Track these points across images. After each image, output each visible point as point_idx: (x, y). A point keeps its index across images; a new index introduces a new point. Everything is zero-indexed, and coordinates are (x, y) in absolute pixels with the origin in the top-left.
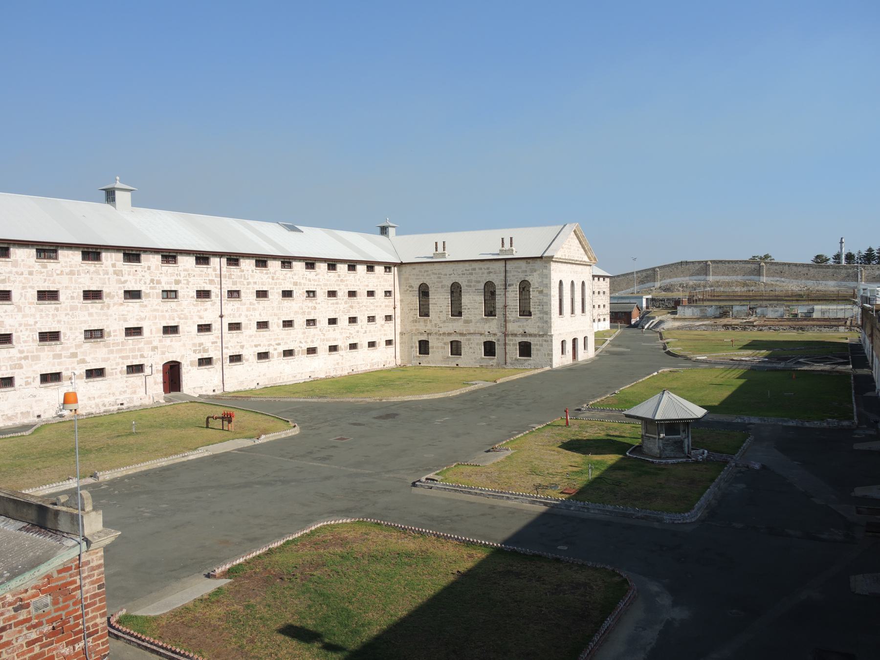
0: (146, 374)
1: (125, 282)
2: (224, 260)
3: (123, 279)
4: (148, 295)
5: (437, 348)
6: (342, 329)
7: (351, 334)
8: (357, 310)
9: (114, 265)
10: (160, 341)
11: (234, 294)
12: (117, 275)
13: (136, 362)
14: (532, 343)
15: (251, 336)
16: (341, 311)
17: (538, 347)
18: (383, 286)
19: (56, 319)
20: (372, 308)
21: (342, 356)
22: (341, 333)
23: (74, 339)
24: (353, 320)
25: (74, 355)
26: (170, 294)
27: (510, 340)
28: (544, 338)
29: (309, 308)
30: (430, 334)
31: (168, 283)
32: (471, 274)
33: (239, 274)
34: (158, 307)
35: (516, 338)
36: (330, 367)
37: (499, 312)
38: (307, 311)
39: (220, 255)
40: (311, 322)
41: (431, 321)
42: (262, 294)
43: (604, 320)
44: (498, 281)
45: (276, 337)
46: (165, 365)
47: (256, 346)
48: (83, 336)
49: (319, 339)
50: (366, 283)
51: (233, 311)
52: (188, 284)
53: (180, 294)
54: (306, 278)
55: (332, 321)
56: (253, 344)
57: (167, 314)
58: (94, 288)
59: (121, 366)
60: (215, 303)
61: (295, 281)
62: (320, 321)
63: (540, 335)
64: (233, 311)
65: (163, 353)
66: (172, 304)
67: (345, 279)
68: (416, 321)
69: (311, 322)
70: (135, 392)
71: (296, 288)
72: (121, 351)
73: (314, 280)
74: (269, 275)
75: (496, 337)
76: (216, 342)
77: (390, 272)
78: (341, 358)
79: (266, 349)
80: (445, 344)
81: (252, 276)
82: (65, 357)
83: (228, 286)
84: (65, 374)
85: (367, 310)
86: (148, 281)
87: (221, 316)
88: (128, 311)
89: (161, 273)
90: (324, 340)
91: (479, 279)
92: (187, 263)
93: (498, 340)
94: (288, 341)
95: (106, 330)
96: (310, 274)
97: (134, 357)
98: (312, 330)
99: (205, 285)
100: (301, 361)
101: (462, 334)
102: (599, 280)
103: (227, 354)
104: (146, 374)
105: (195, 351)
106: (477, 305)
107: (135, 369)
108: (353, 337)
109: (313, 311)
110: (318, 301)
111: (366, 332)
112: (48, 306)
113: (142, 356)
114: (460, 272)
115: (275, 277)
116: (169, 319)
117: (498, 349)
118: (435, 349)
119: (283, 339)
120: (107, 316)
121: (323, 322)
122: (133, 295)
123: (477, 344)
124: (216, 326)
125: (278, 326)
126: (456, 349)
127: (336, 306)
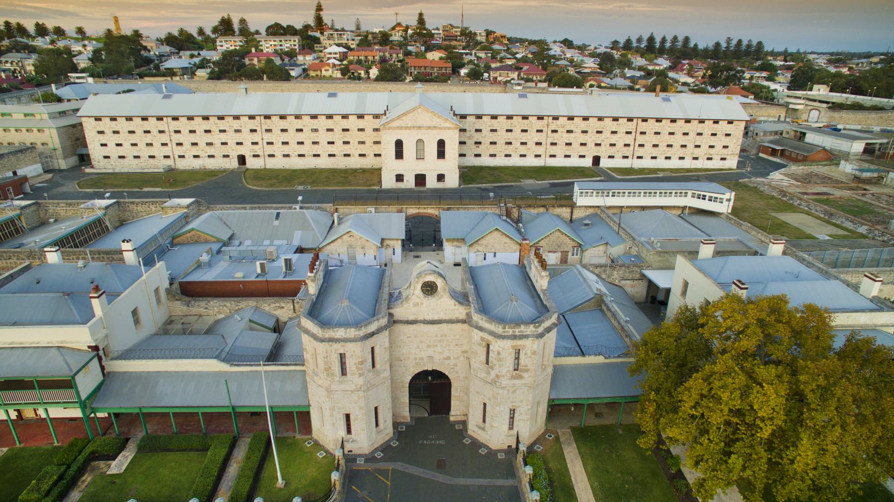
2: (262, 117)
83: (265, 127)
112: (193, 135)
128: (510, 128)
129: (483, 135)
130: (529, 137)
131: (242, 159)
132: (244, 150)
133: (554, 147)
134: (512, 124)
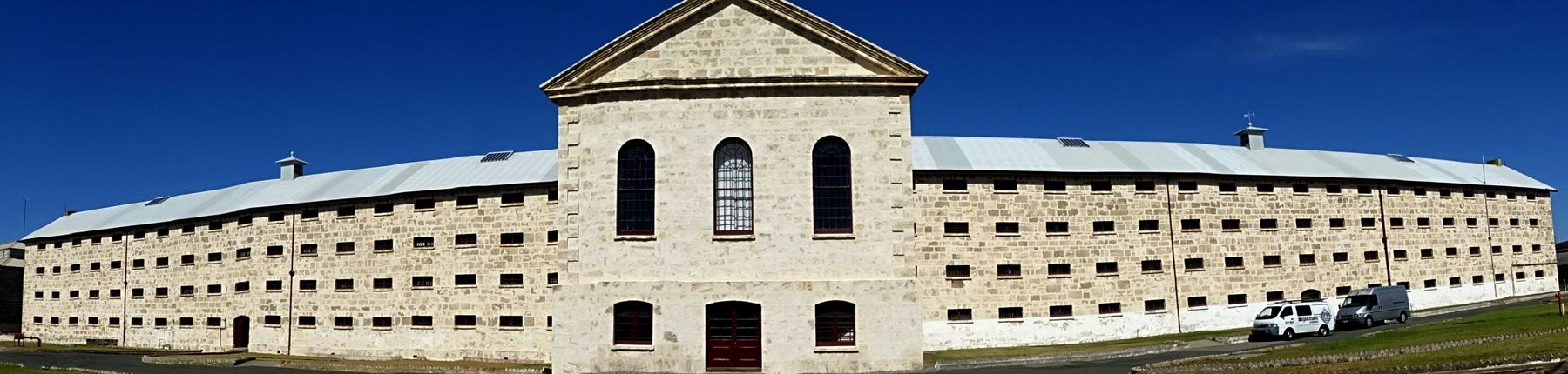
6: (484, 292)
7: (507, 301)
8: (521, 263)
13: (214, 316)
15: (327, 296)
16: (483, 266)
21: (483, 334)
29: (418, 261)
33: (316, 226)
36: (455, 348)
38: (414, 265)
45: (363, 299)
46: (236, 320)
47: (333, 308)
49: (437, 305)
50: (547, 220)
52: (260, 241)
54: (415, 221)
56: (330, 306)
61: (395, 226)
62: (439, 279)
67: (495, 215)
70: (212, 342)
71: (396, 236)
73: (431, 223)
74: (356, 223)
76: (285, 300)
78: (479, 335)
79: (347, 314)
81: (332, 227)
85: (548, 263)
87: (292, 274)
90: (445, 307)
94: (382, 306)
97: (214, 311)
99: (276, 240)
100: (402, 332)
103: (296, 314)
105: (262, 308)
108: (510, 306)
110: (435, 252)
111: (542, 299)
113: (219, 311)
115: (365, 226)
119: (373, 303)
124: (285, 283)
125: (367, 285)
128: (1058, 219)
129: (974, 243)
130: (1120, 246)
131: (242, 325)
132: (252, 306)
133: (1196, 274)
134: (1063, 204)
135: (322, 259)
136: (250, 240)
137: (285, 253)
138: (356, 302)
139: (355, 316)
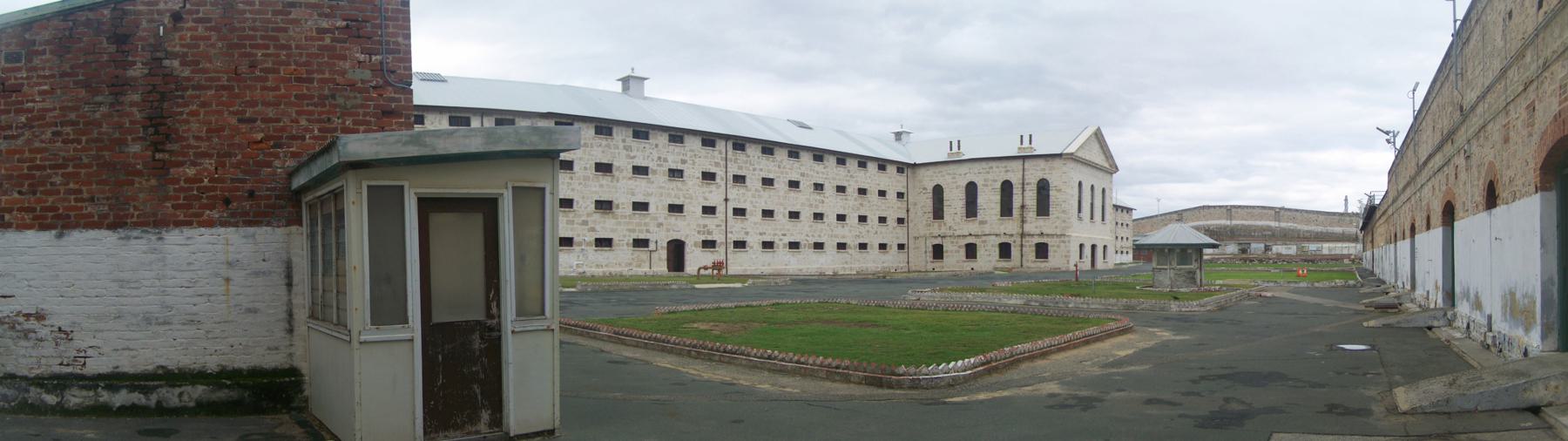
0: (650, 249)
1: (634, 157)
3: (632, 154)
4: (655, 172)
5: (951, 252)
9: (624, 141)
10: (665, 218)
11: (739, 179)
12: (627, 150)
13: (642, 236)
14: (1050, 244)
15: (755, 224)
17: (1055, 248)
18: (896, 186)
19: (570, 187)
20: (883, 208)
22: (850, 231)
23: (586, 208)
24: (863, 219)
25: (585, 223)
26: (676, 174)
27: (1028, 241)
28: (1062, 239)
30: (944, 237)
31: (674, 162)
32: (988, 173)
34: (664, 185)
35: (1033, 239)
37: (1016, 212)
39: (726, 137)
40: (818, 216)
41: (945, 224)
42: (768, 182)
43: (1127, 252)
44: (1015, 179)
46: (669, 243)
47: (761, 234)
48: (593, 206)
51: (738, 197)
53: (685, 174)
55: (841, 218)
56: (758, 232)
57: (673, 193)
58: (605, 161)
59: (627, 238)
60: (720, 186)
63: (1057, 235)
64: (738, 197)
65: (668, 230)
66: (677, 184)
68: (930, 226)
69: (818, 216)
72: (628, 223)
73: (823, 173)
75: (1012, 239)
77: (903, 172)
80: (959, 247)
82: (577, 223)
83: (734, 170)
84: (576, 239)
86: (656, 159)
87: (726, 200)
88: (637, 186)
89: (668, 152)
91: (996, 178)
92: (694, 144)
93: (1014, 242)
95: (615, 202)
96: (818, 167)
97: (641, 231)
98: (819, 225)
101: (977, 236)
102: (1122, 211)
104: (650, 249)
105: (699, 232)
106: (993, 205)
107: (641, 243)
109: (820, 205)
110: (826, 195)
111: (876, 233)
113: (648, 231)
114: (976, 171)
115: (782, 166)
116: (675, 196)
117: (1015, 252)
118: (949, 254)
119: (789, 230)
120: (616, 188)
121: (831, 218)
122: (640, 171)
123: (992, 246)
124: (720, 209)
125: (784, 216)
126: (971, 251)
127: (845, 202)
131: (676, 251)
132: (689, 228)
135: (750, 190)
136: (684, 162)
137: (718, 180)
138: (777, 229)
139: (777, 241)
